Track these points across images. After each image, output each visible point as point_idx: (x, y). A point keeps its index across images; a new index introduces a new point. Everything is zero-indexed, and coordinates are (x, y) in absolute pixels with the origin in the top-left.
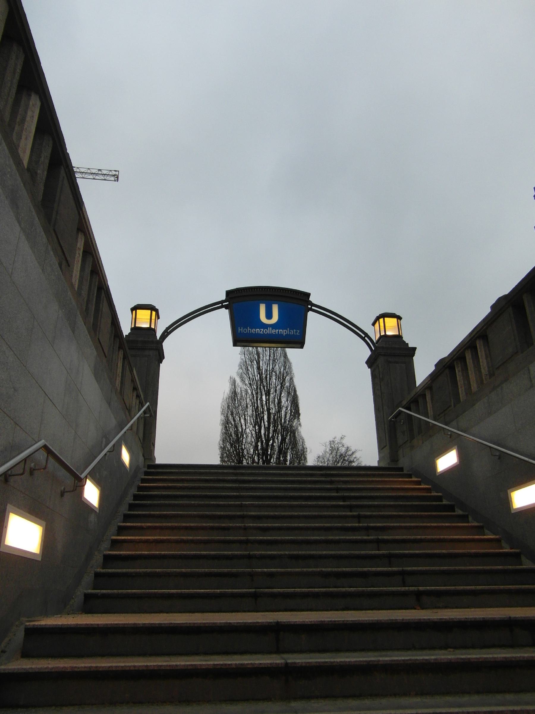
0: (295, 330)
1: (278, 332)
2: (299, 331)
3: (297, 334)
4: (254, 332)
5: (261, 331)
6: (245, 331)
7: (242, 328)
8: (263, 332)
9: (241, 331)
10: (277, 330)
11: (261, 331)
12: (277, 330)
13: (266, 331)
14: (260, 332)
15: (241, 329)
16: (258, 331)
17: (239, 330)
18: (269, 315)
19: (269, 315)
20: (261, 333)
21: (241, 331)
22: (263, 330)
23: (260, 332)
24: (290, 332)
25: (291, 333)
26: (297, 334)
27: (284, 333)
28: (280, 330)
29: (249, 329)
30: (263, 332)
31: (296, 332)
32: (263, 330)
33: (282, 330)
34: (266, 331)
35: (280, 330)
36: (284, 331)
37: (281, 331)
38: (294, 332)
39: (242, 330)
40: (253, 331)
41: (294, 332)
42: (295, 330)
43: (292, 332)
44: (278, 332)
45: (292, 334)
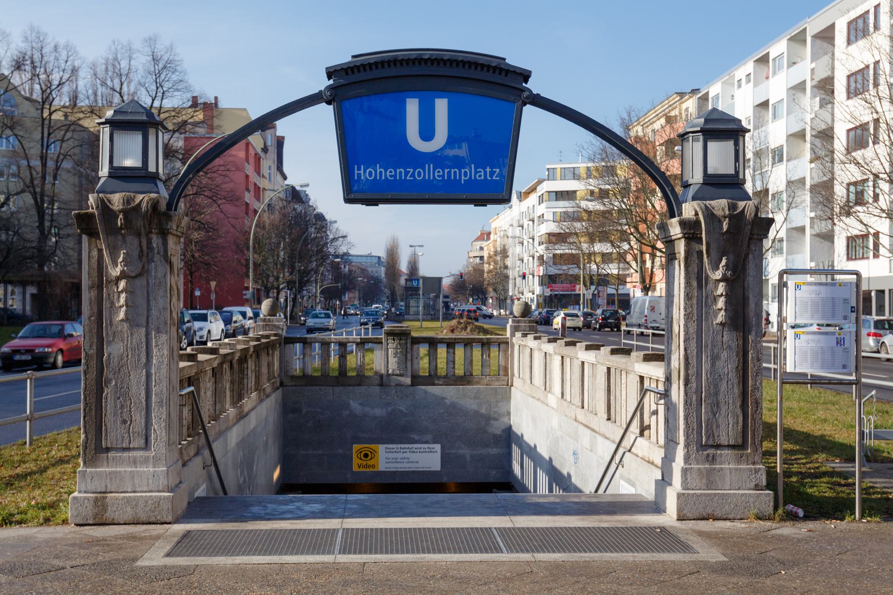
0: (488, 170)
1: (449, 173)
3: (494, 178)
4: (391, 176)
5: (407, 173)
6: (370, 173)
7: (362, 166)
8: (413, 175)
10: (446, 171)
12: (446, 171)
13: (419, 175)
14: (406, 176)
15: (359, 169)
16: (401, 172)
17: (356, 172)
18: (427, 132)
19: (427, 132)
20: (408, 178)
23: (406, 176)
24: (476, 173)
25: (480, 176)
26: (494, 178)
27: (463, 177)
28: (453, 171)
29: (378, 171)
30: (413, 175)
31: (492, 173)
32: (412, 170)
33: (457, 170)
34: (419, 175)
35: (453, 171)
37: (455, 172)
38: (485, 173)
39: (362, 172)
40: (388, 174)
41: (485, 173)
42: (488, 170)
43: (482, 174)
44: (449, 173)
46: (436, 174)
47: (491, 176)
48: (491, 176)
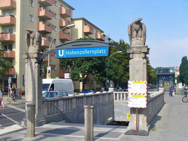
0: (102, 50)
1: (91, 52)
2: (105, 50)
3: (104, 52)
5: (80, 52)
8: (81, 53)
9: (67, 53)
10: (91, 51)
11: (80, 52)
12: (91, 51)
13: (83, 53)
16: (78, 52)
21: (67, 53)
22: (81, 51)
25: (100, 52)
26: (104, 52)
27: (95, 53)
28: (92, 51)
29: (72, 52)
30: (81, 53)
31: (103, 51)
32: (81, 51)
34: (83, 53)
36: (95, 51)
38: (102, 52)
39: (68, 53)
40: (75, 53)
42: (102, 50)
43: (101, 51)
44: (91, 52)
45: (101, 53)
46: (88, 52)
47: (103, 52)
48: (103, 52)
